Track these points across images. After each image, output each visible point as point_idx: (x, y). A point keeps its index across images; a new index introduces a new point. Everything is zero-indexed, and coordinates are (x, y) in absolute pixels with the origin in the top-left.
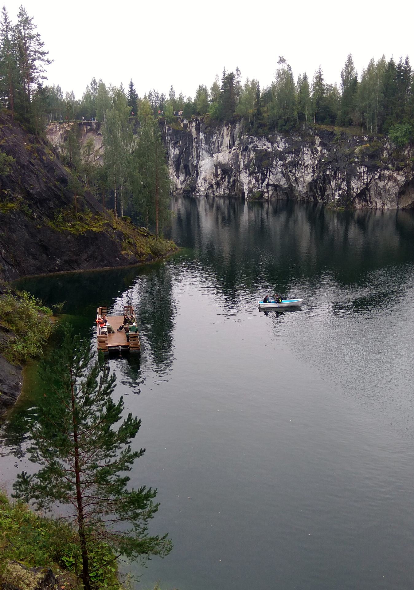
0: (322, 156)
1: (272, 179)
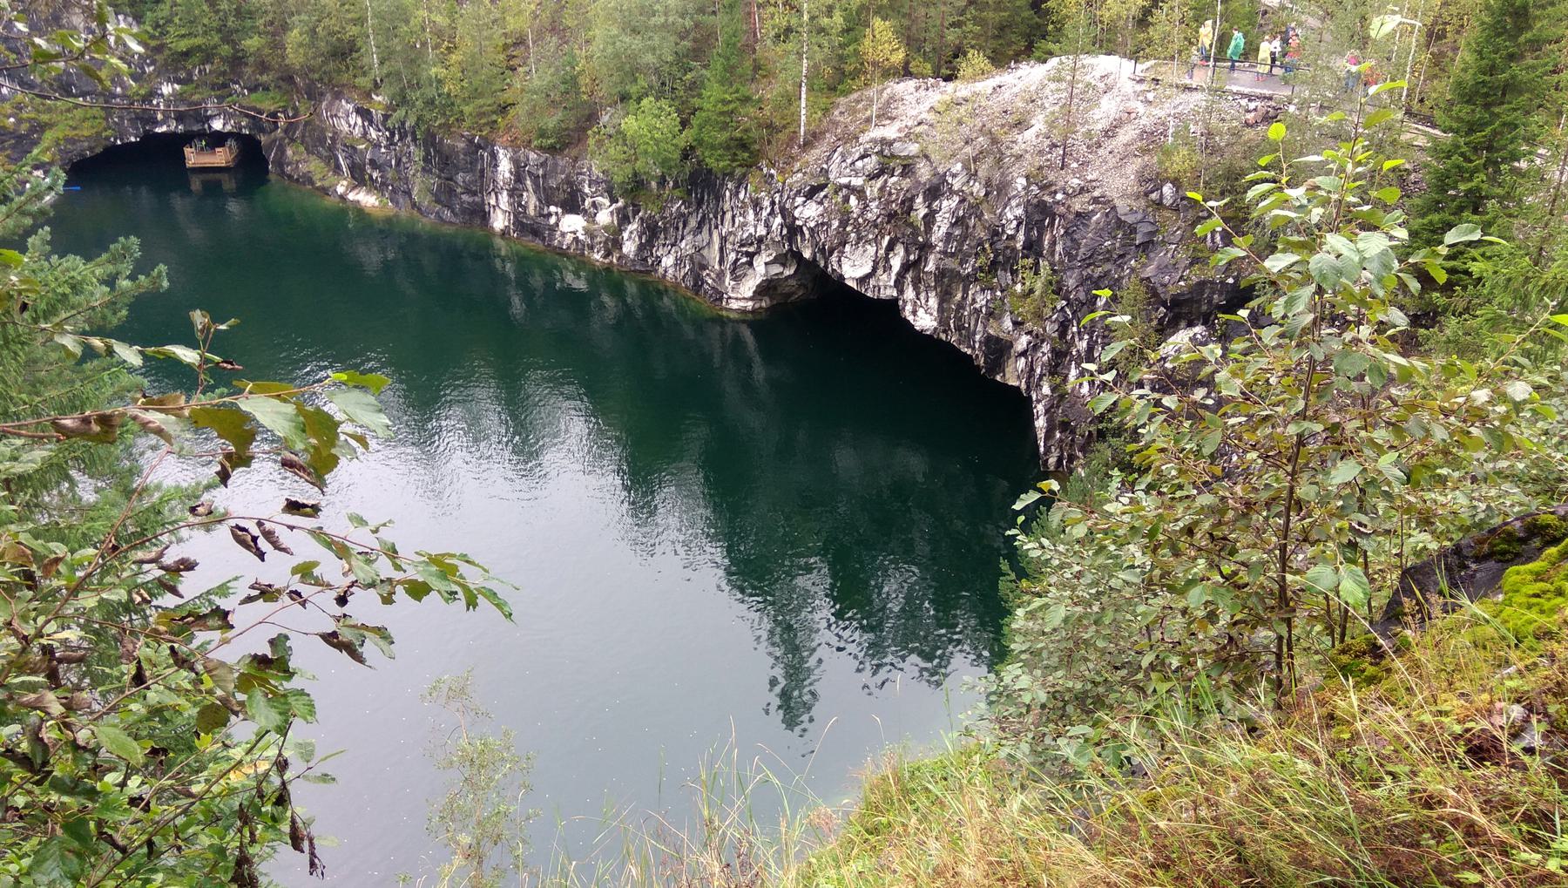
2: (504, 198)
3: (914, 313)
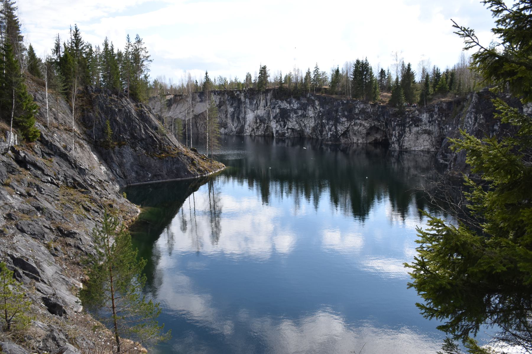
0: (320, 111)
1: (290, 125)
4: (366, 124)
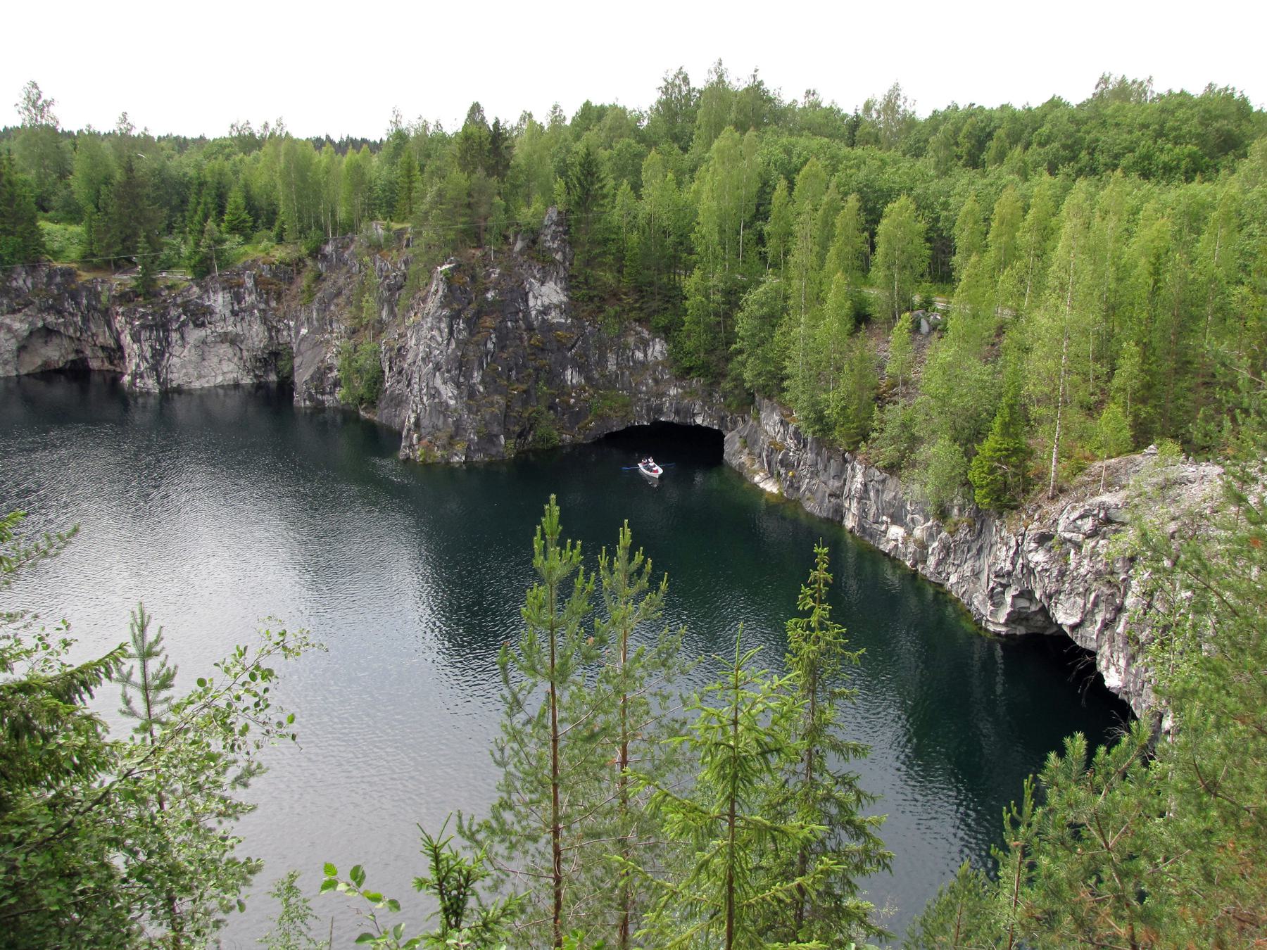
2: (854, 504)
3: (1107, 668)
4: (17, 325)
